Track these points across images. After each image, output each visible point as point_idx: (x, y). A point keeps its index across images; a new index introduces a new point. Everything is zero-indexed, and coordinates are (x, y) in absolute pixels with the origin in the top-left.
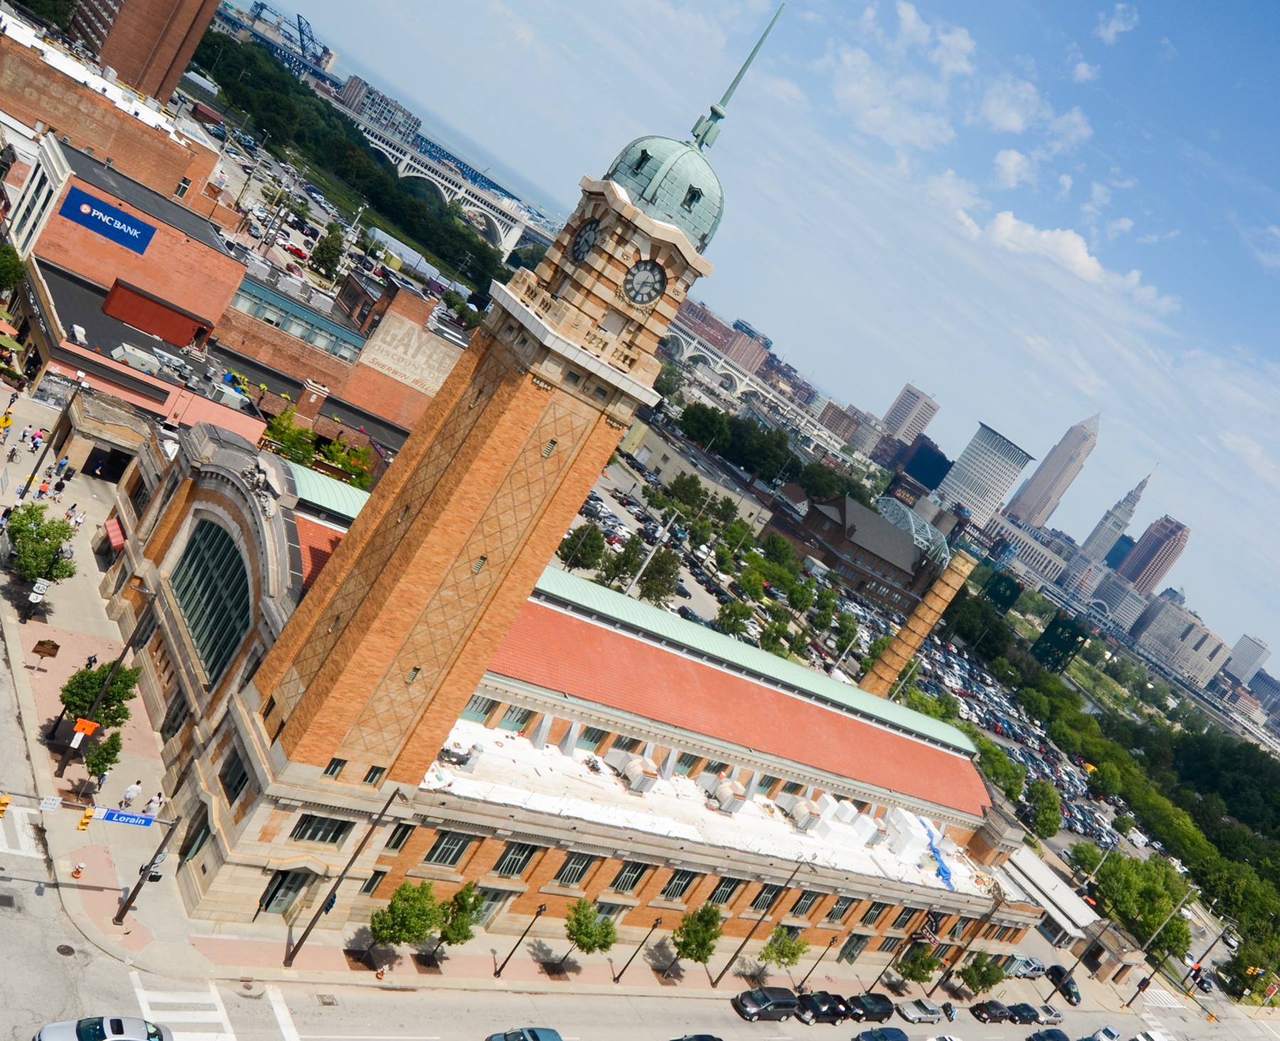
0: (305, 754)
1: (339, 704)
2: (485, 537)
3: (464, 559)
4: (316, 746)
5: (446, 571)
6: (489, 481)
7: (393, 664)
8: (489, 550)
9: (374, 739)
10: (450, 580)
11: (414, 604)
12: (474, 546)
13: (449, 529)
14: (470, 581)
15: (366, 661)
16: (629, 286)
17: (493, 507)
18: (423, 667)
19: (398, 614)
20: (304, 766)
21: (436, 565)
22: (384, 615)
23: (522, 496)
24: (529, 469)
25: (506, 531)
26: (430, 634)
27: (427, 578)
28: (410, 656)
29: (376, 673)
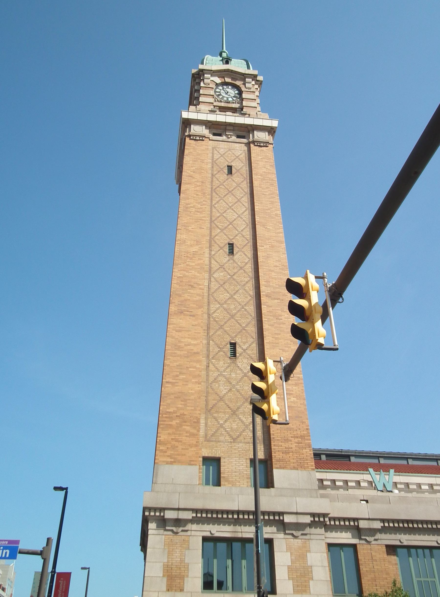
0: (169, 453)
1: (177, 389)
2: (222, 230)
3: (215, 248)
4: (177, 441)
5: (207, 259)
6: (200, 194)
7: (208, 344)
8: (231, 237)
9: (235, 426)
10: (215, 266)
11: (195, 285)
12: (217, 237)
13: (190, 228)
14: (231, 261)
15: (180, 342)
16: (221, 97)
17: (214, 210)
18: (238, 340)
19: (186, 296)
20: (175, 467)
21: (195, 253)
22: (175, 300)
23: (230, 199)
24: (224, 184)
25: (235, 222)
26: (225, 309)
27: (194, 264)
28: (219, 332)
29: (195, 350)
